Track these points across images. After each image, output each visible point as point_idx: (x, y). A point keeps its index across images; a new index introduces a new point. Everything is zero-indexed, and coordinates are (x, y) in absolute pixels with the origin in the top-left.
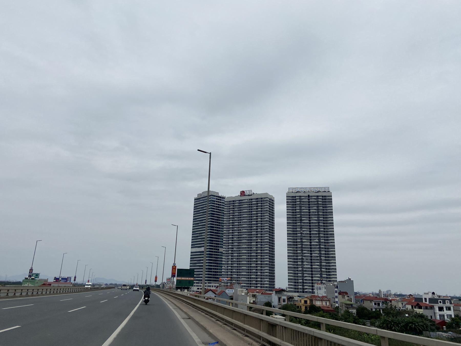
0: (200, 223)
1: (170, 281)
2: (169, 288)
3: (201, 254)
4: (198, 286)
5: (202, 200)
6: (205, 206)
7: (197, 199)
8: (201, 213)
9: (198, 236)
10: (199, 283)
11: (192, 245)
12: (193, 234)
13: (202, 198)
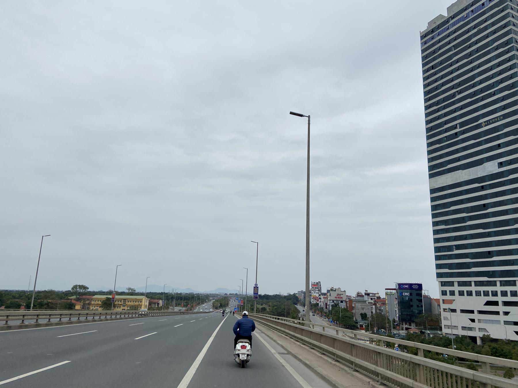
0: (460, 92)
1: (317, 288)
2: (335, 299)
3: (482, 187)
4: (488, 295)
5: (454, 24)
6: (475, 30)
7: (433, 31)
8: (457, 61)
9: (456, 135)
10: (494, 284)
11: (431, 168)
12: (428, 137)
13: (453, 17)
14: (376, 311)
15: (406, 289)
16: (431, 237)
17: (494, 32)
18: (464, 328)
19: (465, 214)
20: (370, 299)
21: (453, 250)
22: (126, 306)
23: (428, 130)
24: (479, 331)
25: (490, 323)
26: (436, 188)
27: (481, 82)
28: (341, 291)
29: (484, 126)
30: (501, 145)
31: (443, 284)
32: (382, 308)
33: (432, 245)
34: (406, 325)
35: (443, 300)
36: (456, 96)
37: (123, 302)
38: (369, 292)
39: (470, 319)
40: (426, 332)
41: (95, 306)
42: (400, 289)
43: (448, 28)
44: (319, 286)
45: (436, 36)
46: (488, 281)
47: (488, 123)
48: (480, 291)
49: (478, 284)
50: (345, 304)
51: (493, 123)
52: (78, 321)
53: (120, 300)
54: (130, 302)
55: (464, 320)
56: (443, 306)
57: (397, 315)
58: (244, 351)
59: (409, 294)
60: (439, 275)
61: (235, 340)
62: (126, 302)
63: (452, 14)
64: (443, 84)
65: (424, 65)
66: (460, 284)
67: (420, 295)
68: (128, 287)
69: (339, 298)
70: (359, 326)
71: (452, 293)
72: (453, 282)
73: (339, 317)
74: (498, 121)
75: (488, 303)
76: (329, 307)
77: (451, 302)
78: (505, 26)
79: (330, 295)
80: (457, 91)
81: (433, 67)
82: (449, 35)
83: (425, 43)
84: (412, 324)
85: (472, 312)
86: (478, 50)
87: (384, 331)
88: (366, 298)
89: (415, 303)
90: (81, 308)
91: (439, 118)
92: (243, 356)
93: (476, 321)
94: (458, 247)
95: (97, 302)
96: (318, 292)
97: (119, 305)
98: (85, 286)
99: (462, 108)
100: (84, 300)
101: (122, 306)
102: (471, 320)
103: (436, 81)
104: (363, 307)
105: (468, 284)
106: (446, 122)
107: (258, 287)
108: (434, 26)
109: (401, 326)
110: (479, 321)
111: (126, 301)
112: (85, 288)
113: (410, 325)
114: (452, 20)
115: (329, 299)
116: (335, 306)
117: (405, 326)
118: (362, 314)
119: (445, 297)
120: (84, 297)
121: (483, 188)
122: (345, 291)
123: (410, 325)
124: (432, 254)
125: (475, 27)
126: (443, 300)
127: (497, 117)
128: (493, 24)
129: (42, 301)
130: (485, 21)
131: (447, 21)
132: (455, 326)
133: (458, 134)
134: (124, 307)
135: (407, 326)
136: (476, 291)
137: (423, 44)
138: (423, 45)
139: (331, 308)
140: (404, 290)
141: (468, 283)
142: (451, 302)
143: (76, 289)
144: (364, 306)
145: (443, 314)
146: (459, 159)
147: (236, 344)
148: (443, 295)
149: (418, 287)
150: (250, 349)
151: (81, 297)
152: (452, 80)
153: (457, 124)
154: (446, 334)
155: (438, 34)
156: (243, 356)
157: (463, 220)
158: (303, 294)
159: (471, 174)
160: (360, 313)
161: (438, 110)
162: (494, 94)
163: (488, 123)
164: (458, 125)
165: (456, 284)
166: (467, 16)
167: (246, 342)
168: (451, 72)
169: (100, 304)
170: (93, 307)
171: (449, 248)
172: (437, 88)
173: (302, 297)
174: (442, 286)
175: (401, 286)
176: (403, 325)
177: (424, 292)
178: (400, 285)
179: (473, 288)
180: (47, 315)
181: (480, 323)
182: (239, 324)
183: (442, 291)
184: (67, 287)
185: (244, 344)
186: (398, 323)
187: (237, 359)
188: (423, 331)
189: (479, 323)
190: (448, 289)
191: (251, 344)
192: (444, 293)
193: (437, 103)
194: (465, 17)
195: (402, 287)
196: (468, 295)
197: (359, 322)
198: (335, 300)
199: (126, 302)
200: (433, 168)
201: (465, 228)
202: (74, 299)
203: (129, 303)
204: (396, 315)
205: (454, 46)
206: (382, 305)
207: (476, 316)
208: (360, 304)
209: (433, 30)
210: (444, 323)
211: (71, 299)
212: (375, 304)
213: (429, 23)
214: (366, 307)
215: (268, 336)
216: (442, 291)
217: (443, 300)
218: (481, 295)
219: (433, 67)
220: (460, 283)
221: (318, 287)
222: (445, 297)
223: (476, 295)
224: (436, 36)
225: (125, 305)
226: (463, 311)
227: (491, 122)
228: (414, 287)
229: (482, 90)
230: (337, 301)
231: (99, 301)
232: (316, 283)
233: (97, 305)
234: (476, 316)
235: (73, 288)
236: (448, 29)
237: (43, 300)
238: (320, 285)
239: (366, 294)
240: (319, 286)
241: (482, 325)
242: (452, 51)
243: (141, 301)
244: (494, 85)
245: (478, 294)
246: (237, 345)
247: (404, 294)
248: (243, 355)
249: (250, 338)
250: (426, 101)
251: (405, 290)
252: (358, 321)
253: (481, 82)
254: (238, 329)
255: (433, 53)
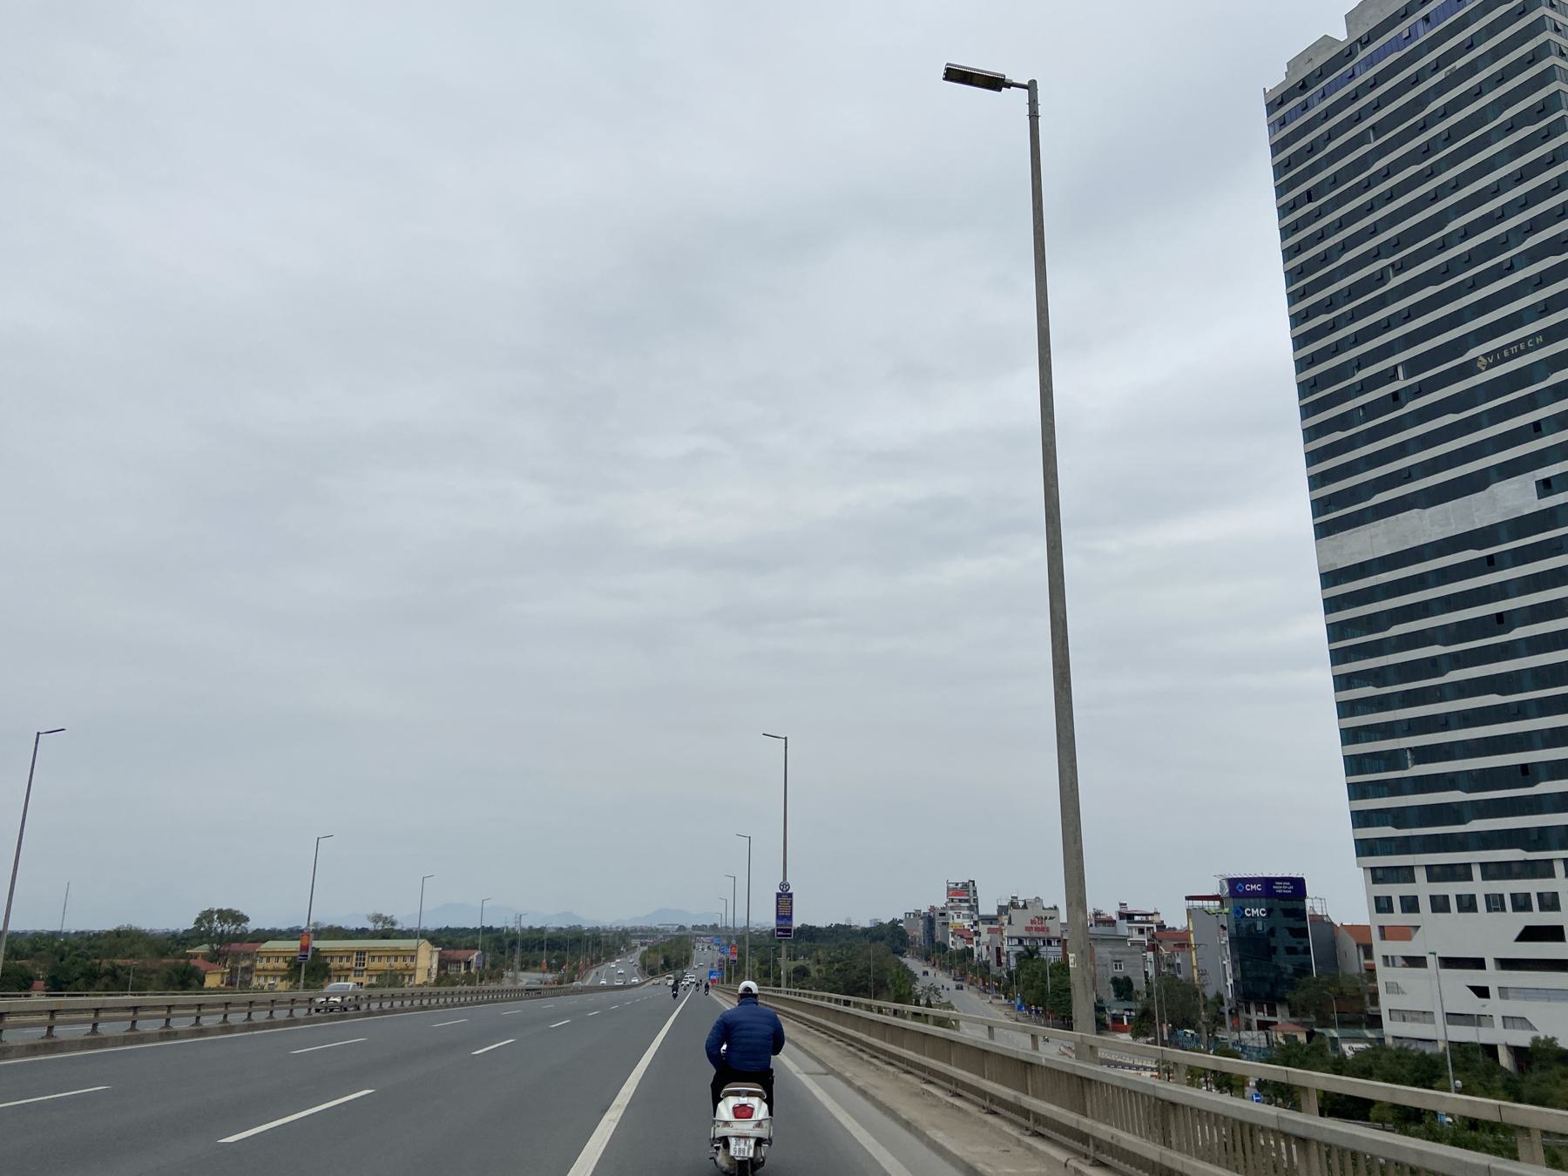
0: (1400, 268)
1: (966, 901)
2: (1026, 934)
3: (1490, 559)
5: (1370, 62)
6: (1440, 76)
7: (1304, 86)
8: (1388, 173)
9: (1396, 399)
11: (1319, 507)
12: (1307, 411)
13: (1364, 42)
14: (1158, 972)
15: (1254, 894)
16: (1331, 725)
17: (1501, 78)
18: (1454, 1018)
19: (1437, 646)
20: (1135, 933)
21: (1407, 765)
22: (365, 973)
23: (1305, 388)
24: (1505, 1027)
25: (1539, 999)
26: (1339, 567)
27: (1466, 233)
28: (1044, 909)
29: (1483, 368)
30: (1543, 427)
31: (1379, 876)
32: (1178, 961)
33: (1334, 752)
34: (1261, 1014)
35: (1380, 927)
36: (1390, 280)
37: (357, 959)
38: (1131, 908)
39: (1469, 987)
40: (1327, 1035)
41: (266, 977)
42: (1233, 897)
43: (1353, 75)
44: (971, 895)
45: (1316, 100)
46: (1525, 862)
47: (1497, 357)
48: (1501, 896)
49: (1493, 871)
50: (1060, 949)
51: (1512, 357)
52: (94, 1037)
53: (346, 954)
54: (376, 959)
55: (1455, 989)
56: (1380, 948)
57: (1230, 981)
58: (745, 1127)
59: (1263, 912)
60: (1365, 848)
61: (712, 1085)
62: (364, 959)
63: (1361, 31)
64: (1345, 246)
65: (1281, 190)
66: (1435, 874)
67: (1300, 914)
68: (371, 912)
69: (1037, 929)
70: (1109, 1021)
71: (1410, 905)
72: (1413, 866)
73: (1043, 992)
74: (1527, 351)
75: (1529, 934)
76: (1008, 960)
77: (1405, 933)
78: (1532, 59)
79: (1010, 923)
80: (1392, 265)
81: (1309, 196)
82: (1355, 96)
83: (1283, 123)
84: (1278, 1009)
85: (1479, 964)
86: (1450, 136)
87: (1192, 1035)
88: (1123, 927)
89: (1283, 940)
90: (222, 982)
91: (1337, 349)
92: (742, 1146)
93: (1493, 992)
94: (1423, 755)
95: (272, 964)
96: (967, 912)
97: (342, 969)
98: (236, 912)
99: (1409, 315)
100: (237, 957)
101: (352, 974)
102: (1473, 989)
103: (1322, 236)
104: (1117, 958)
105: (1462, 872)
106: (1361, 363)
107: (790, 895)
108: (1307, 70)
109: (1243, 1014)
110: (1504, 992)
111: (367, 957)
112: (237, 918)
113: (1272, 1013)
114: (1363, 48)
115: (1006, 934)
116: (1029, 956)
117: (1256, 1016)
118: (1115, 981)
119: (1387, 920)
120: (235, 947)
121: (1491, 564)
122: (1056, 908)
123: (1272, 1013)
124: (1338, 781)
125: (1437, 66)
126: (1382, 928)
127: (1525, 339)
128: (1496, 54)
129: (94, 965)
130: (1470, 45)
131: (1349, 53)
132: (1424, 1012)
133: (1402, 397)
134: (359, 976)
135: (1263, 1016)
136: (1487, 896)
137: (1277, 126)
138: (1277, 130)
139: (1013, 963)
140: (1246, 901)
141: (1461, 870)
142: (1405, 933)
143: (212, 921)
144: (1122, 953)
145: (1384, 975)
146: (1410, 476)
147: (716, 1100)
148: (1379, 910)
149: (1291, 887)
150: (768, 1117)
151: (226, 949)
152: (1373, 231)
153: (1396, 367)
154: (1395, 1038)
155: (1321, 94)
156: (742, 1146)
157: (1433, 666)
158: (921, 922)
159: (1452, 520)
160: (1110, 979)
161: (1333, 326)
162: (1511, 268)
163: (1497, 357)
164: (1400, 370)
165: (1421, 875)
166: (1410, 36)
167: (750, 1094)
168: (1370, 208)
169: (284, 970)
170: (262, 981)
171: (1393, 760)
172: (1325, 258)
173: (917, 931)
174: (1375, 880)
175: (1237, 887)
176: (1248, 1012)
177: (1312, 905)
178: (1233, 882)
179: (1478, 887)
180: (87, 1010)
181: (1507, 998)
182: (726, 1029)
183: (1377, 899)
184: (182, 920)
185: (744, 1100)
186: (1234, 1004)
187: (721, 1158)
188: (1316, 1030)
189: (1504, 1001)
190: (1396, 891)
191: (769, 1101)
192: (1383, 905)
193: (1329, 305)
194: (1404, 37)
195: (1241, 891)
196: (1461, 910)
197: (1109, 1007)
198: (1026, 938)
199: (366, 962)
200: (1326, 506)
201: (1441, 693)
202: (204, 956)
203: (376, 964)
204: (1226, 980)
205: (1373, 127)
206: (1178, 949)
207: (1491, 977)
208: (1109, 949)
209: (1304, 82)
210: (1386, 1002)
211: (195, 956)
212: (1154, 948)
213: (1292, 65)
214: (1127, 956)
215: (863, 1092)
216: (1377, 899)
217: (1382, 928)
218: (1504, 910)
219: (1309, 196)
220: (1437, 870)
221: (967, 898)
222: (1387, 920)
223: (1489, 910)
224: (1316, 100)
225: (362, 971)
226: (1448, 963)
227: (1506, 354)
228: (1278, 888)
229: (1470, 259)
230: (1032, 939)
231: (281, 960)
232: (960, 885)
233: (274, 973)
234: (1491, 977)
235: (199, 921)
236: (1352, 76)
237: (97, 961)
238: (975, 891)
239: (1122, 916)
240: (971, 894)
241: (1514, 1007)
242: (1370, 143)
243: (412, 957)
244: (1508, 240)
245: (1495, 903)
246: (719, 1105)
247: (1248, 912)
248: (742, 1141)
249: (764, 1079)
250: (1293, 298)
251: (1252, 901)
252: (1106, 1004)
253: (1466, 233)
254: (724, 1047)
255: (1309, 152)
